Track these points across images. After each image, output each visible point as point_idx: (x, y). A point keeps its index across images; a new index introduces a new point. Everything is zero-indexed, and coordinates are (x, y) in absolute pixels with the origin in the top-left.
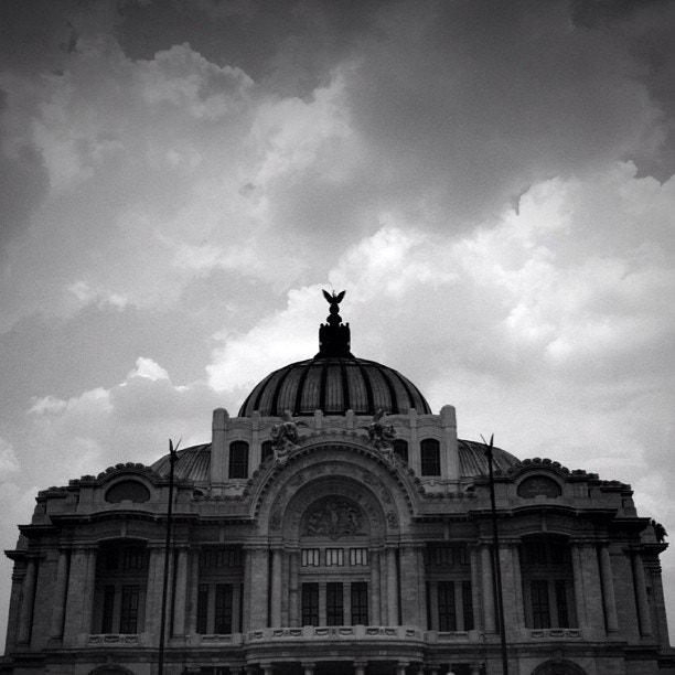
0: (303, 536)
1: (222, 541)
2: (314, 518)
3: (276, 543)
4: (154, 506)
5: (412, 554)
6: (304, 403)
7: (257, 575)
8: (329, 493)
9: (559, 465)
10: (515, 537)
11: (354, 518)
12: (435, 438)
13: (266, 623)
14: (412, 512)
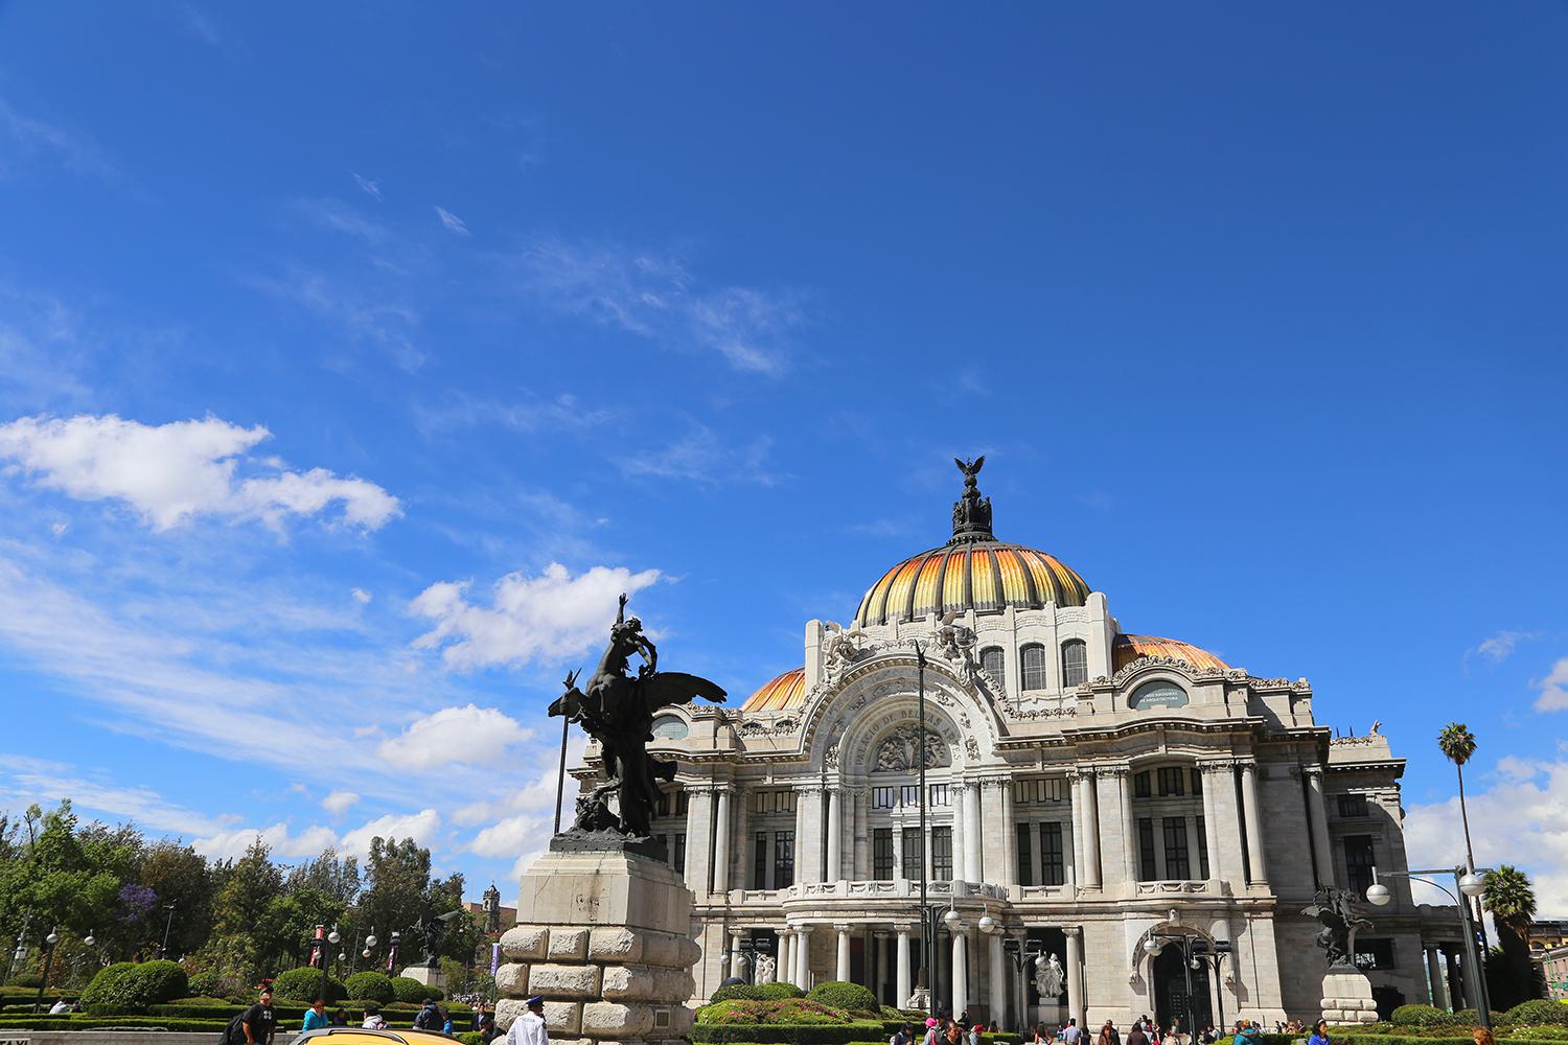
4: (691, 742)
6: (917, 605)
10: (1124, 762)
11: (935, 747)
12: (1078, 637)
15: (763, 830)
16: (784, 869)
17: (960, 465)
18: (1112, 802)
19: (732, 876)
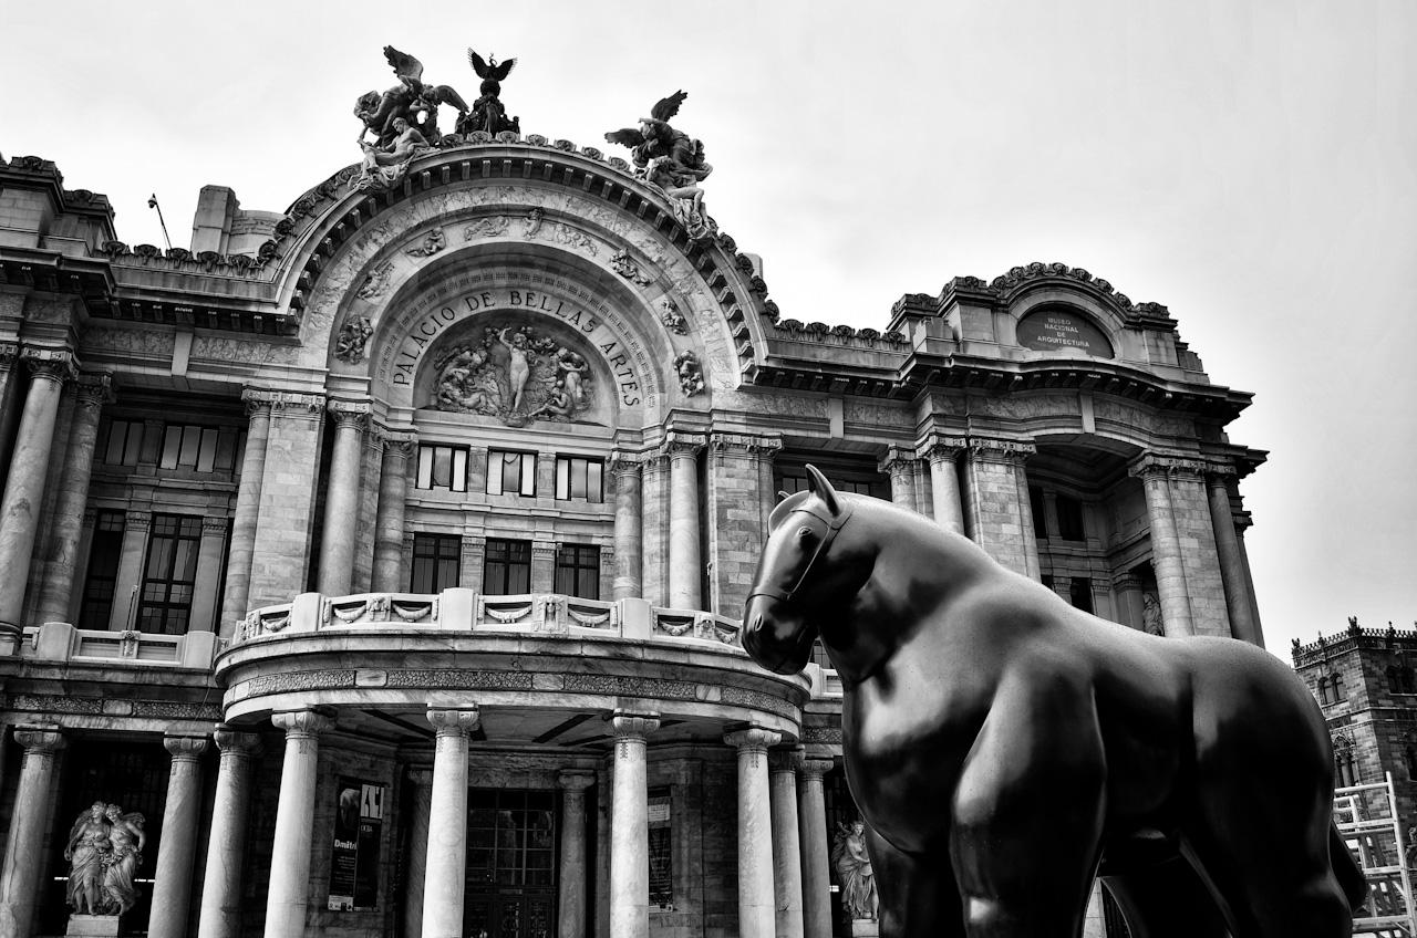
0: (424, 408)
1: (179, 367)
2: (462, 364)
3: (353, 396)
5: (743, 465)
7: (279, 474)
8: (501, 303)
9: (1108, 288)
10: (1025, 438)
11: (571, 379)
13: (299, 580)
14: (749, 353)
15: (123, 506)
16: (166, 605)
17: (477, 61)
18: (1004, 509)
19: (36, 589)
